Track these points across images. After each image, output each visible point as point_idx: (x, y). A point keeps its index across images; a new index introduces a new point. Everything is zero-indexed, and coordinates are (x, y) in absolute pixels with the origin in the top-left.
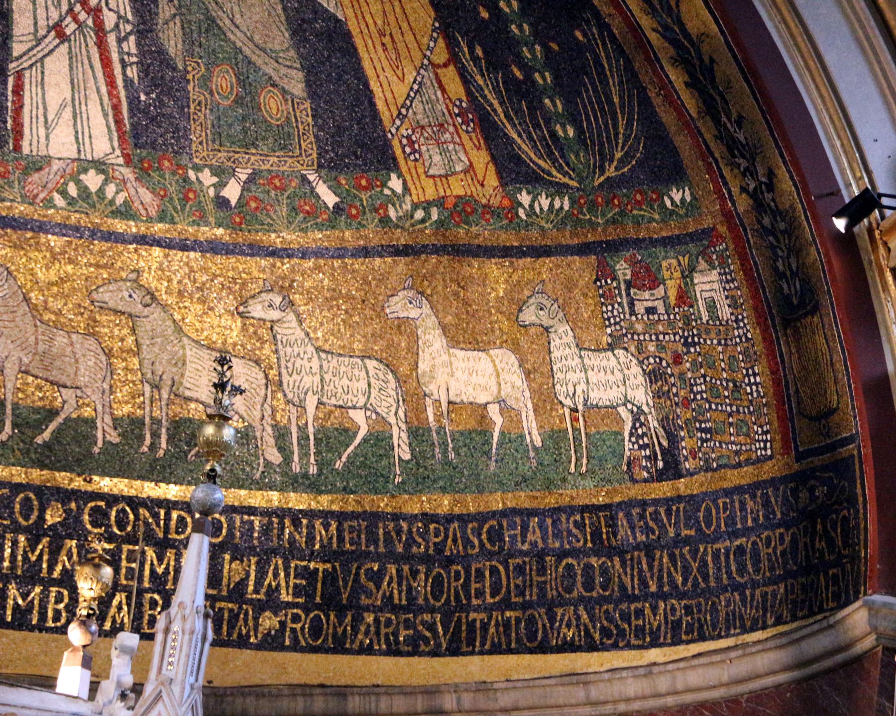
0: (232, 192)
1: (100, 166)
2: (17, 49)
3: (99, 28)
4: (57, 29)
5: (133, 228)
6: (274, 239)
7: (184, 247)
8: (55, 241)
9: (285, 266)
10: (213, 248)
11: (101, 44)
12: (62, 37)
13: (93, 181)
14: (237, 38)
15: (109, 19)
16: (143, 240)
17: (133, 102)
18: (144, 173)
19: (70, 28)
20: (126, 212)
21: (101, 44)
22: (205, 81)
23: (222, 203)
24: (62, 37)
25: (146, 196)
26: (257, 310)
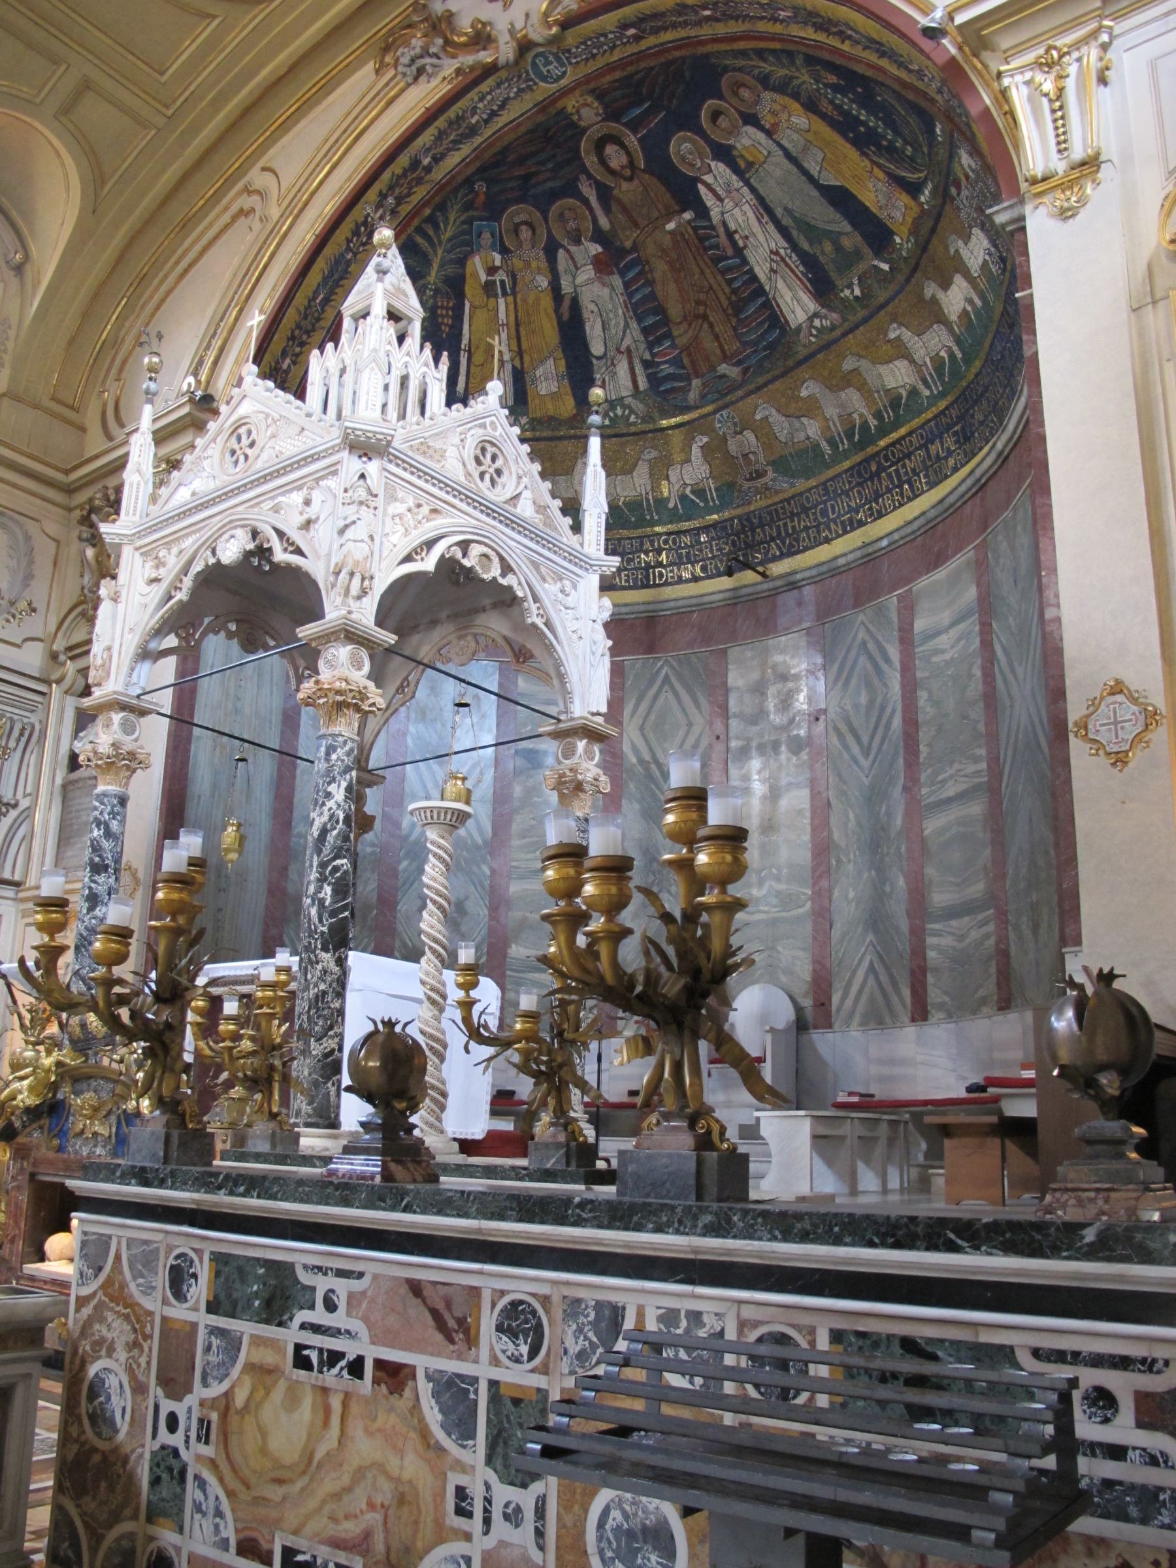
0: (857, 292)
1: (816, 315)
2: (767, 288)
3: (783, 260)
4: (772, 270)
5: (838, 332)
6: (882, 300)
7: (856, 327)
8: (820, 356)
9: (890, 308)
10: (865, 321)
11: (787, 265)
12: (775, 272)
13: (817, 323)
14: (821, 226)
15: (782, 252)
16: (845, 334)
17: (809, 280)
18: (831, 309)
19: (775, 266)
20: (833, 328)
21: (787, 265)
22: (823, 252)
23: (857, 298)
24: (775, 272)
25: (834, 315)
26: (892, 335)
